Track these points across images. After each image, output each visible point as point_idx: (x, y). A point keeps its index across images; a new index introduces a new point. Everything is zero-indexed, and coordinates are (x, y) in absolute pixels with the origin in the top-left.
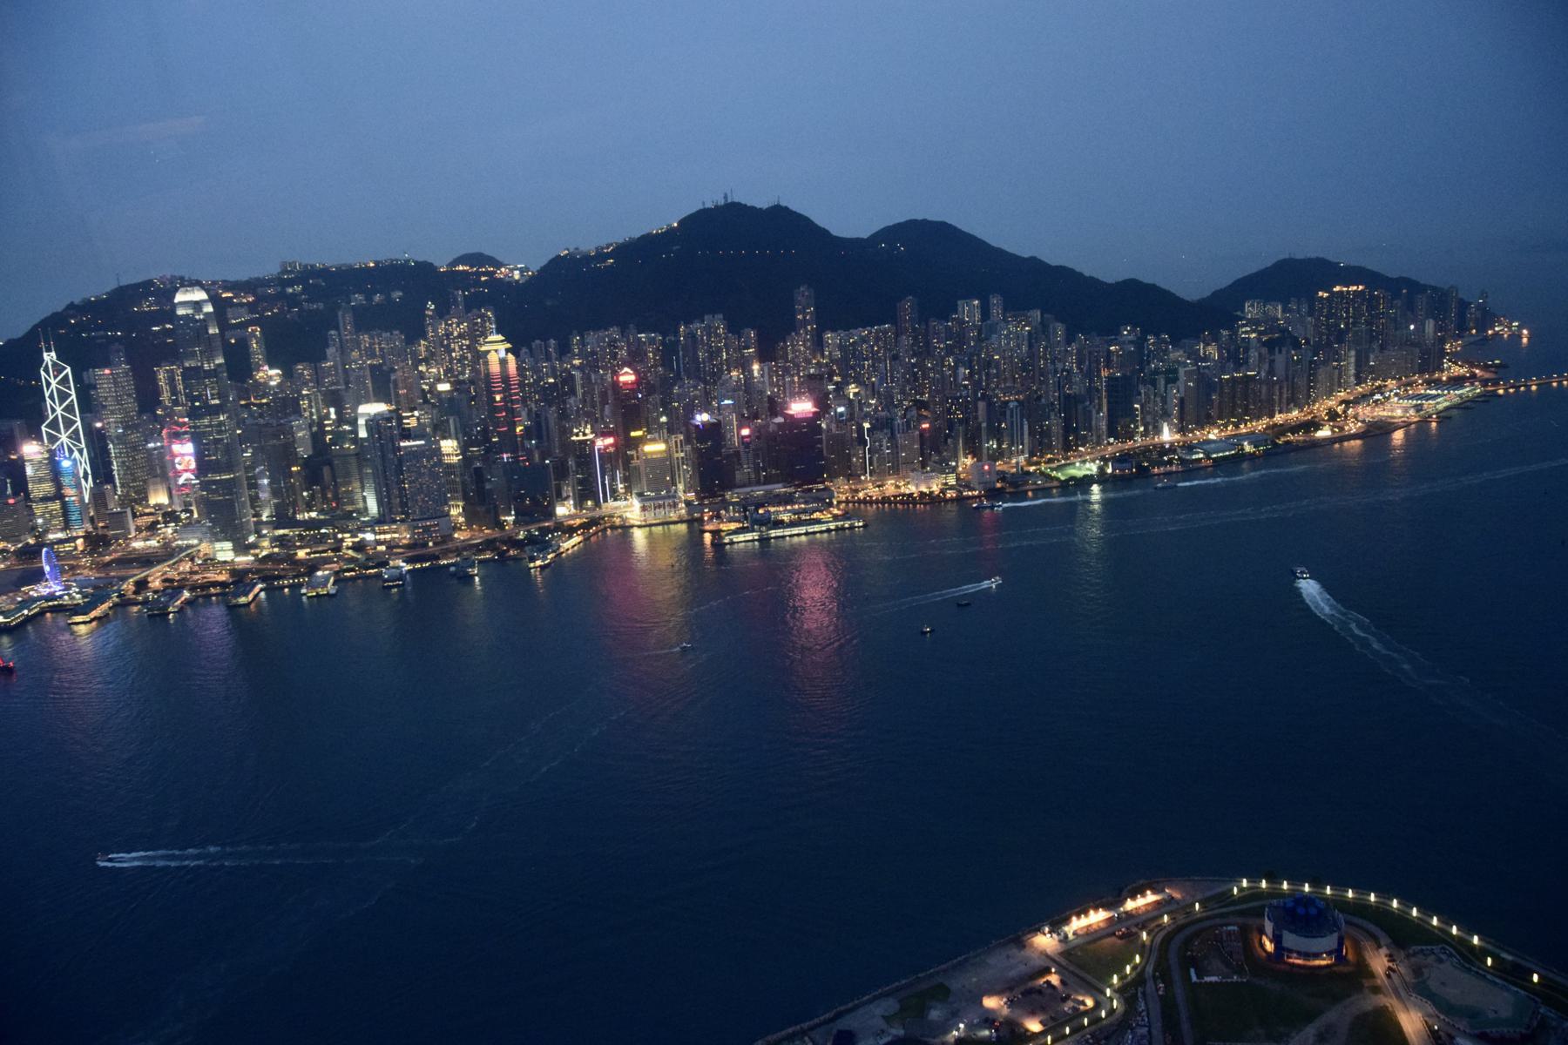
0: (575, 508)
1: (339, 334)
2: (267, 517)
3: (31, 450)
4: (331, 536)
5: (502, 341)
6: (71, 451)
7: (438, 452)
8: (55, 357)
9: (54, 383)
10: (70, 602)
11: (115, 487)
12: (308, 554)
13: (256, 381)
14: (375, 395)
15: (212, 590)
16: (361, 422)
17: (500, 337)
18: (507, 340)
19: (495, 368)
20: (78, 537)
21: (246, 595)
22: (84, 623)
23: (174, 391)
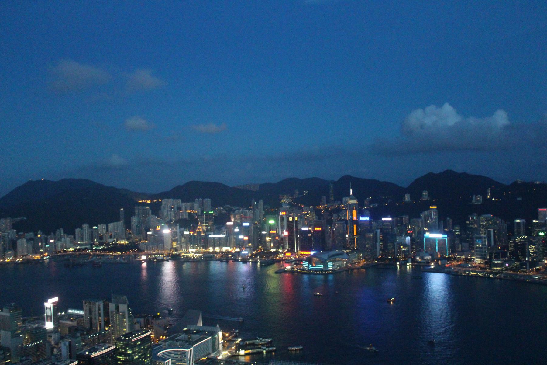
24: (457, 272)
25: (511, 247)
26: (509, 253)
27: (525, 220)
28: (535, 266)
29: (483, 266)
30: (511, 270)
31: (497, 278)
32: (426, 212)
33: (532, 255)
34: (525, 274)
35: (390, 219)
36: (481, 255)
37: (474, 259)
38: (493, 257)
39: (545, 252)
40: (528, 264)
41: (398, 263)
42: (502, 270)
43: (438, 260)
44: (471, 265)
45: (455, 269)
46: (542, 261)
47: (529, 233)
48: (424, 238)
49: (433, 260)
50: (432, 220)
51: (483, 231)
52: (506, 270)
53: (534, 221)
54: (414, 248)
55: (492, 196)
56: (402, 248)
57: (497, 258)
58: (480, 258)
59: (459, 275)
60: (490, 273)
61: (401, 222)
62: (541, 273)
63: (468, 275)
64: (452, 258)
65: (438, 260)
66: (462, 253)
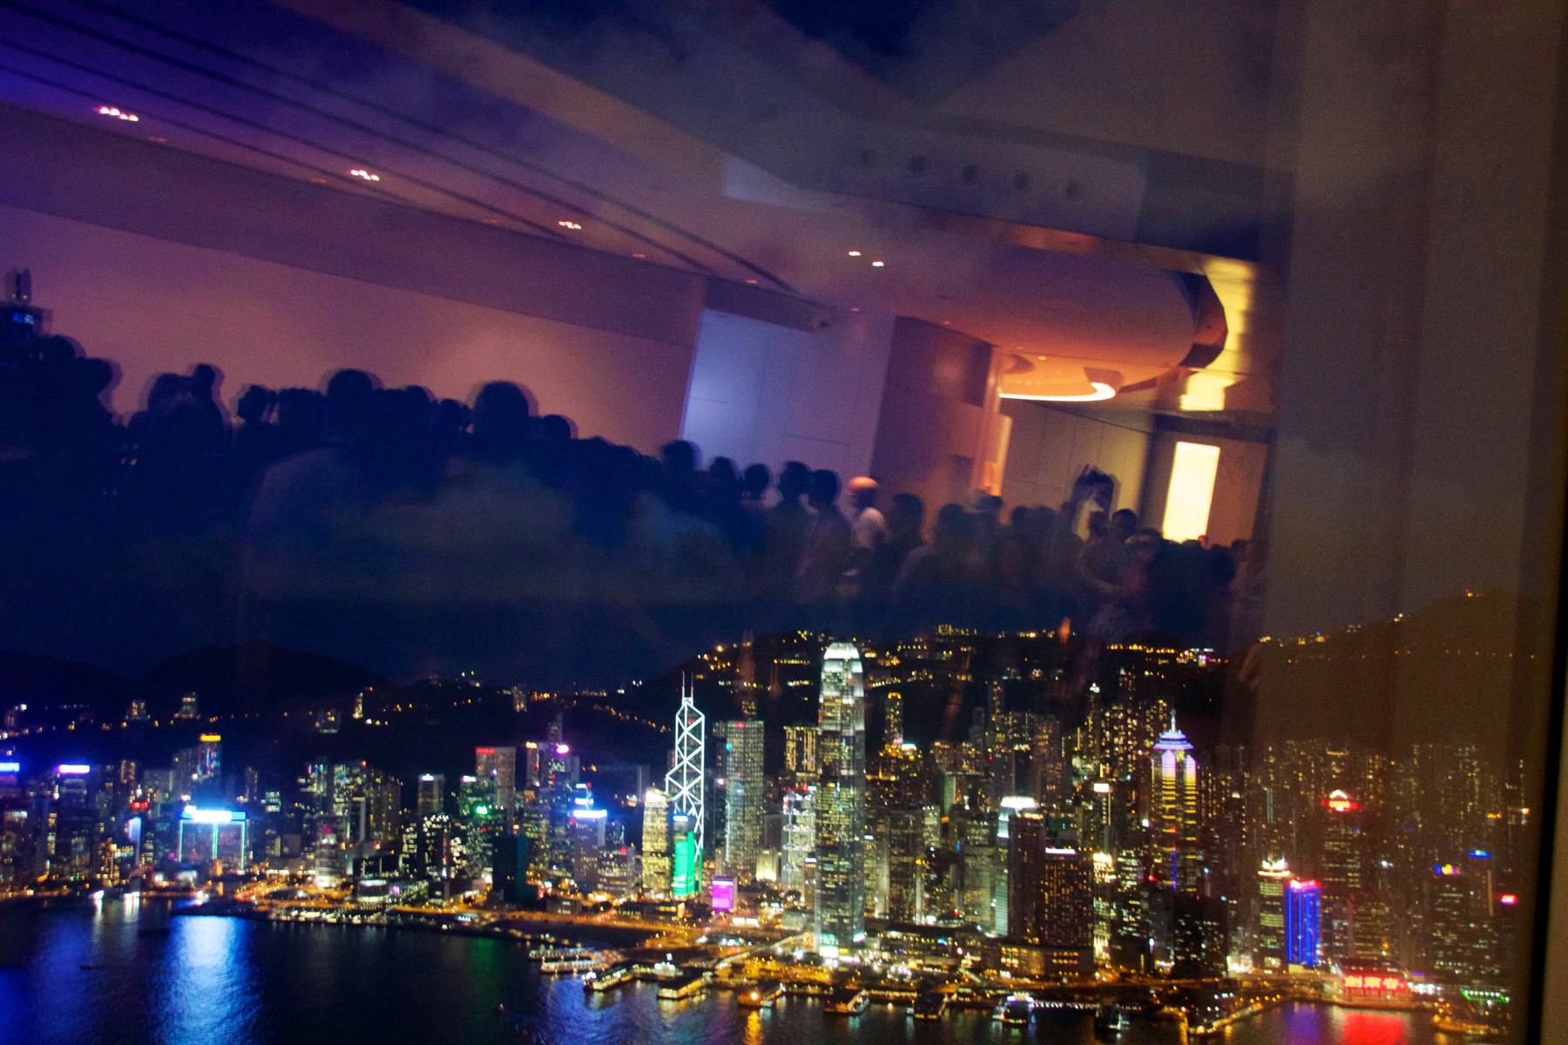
0: (1255, 965)
1: (986, 712)
2: (880, 914)
3: (654, 798)
4: (950, 950)
5: (1181, 740)
6: (689, 806)
7: (1089, 866)
8: (692, 706)
9: (687, 731)
10: (662, 973)
11: (725, 849)
12: (919, 965)
13: (887, 754)
14: (1016, 790)
15: (810, 989)
16: (1003, 818)
17: (1179, 735)
18: (1188, 740)
19: (1169, 772)
20: (680, 902)
21: (846, 1002)
22: (673, 999)
23: (800, 758)
24: (266, 913)
25: (408, 843)
26: (405, 861)
27: (445, 776)
28: (464, 891)
29: (335, 894)
30: (405, 902)
31: (371, 925)
32: (190, 752)
33: (459, 865)
34: (440, 911)
35: (84, 769)
36: (333, 866)
37: (313, 876)
38: (363, 869)
39: (487, 856)
40: (447, 887)
41: (98, 896)
42: (384, 904)
43: (216, 880)
44: (305, 892)
45: (262, 904)
46: (479, 878)
47: (451, 807)
48: (182, 822)
49: (200, 882)
50: (205, 772)
51: (340, 803)
52: (393, 903)
53: (467, 779)
54: (150, 851)
55: (366, 714)
56: (112, 853)
57: (373, 871)
58: (331, 874)
59: (272, 921)
60: (354, 913)
61: (115, 776)
62: (476, 907)
63: (296, 921)
64: (254, 875)
65: (216, 880)
66: (282, 861)
